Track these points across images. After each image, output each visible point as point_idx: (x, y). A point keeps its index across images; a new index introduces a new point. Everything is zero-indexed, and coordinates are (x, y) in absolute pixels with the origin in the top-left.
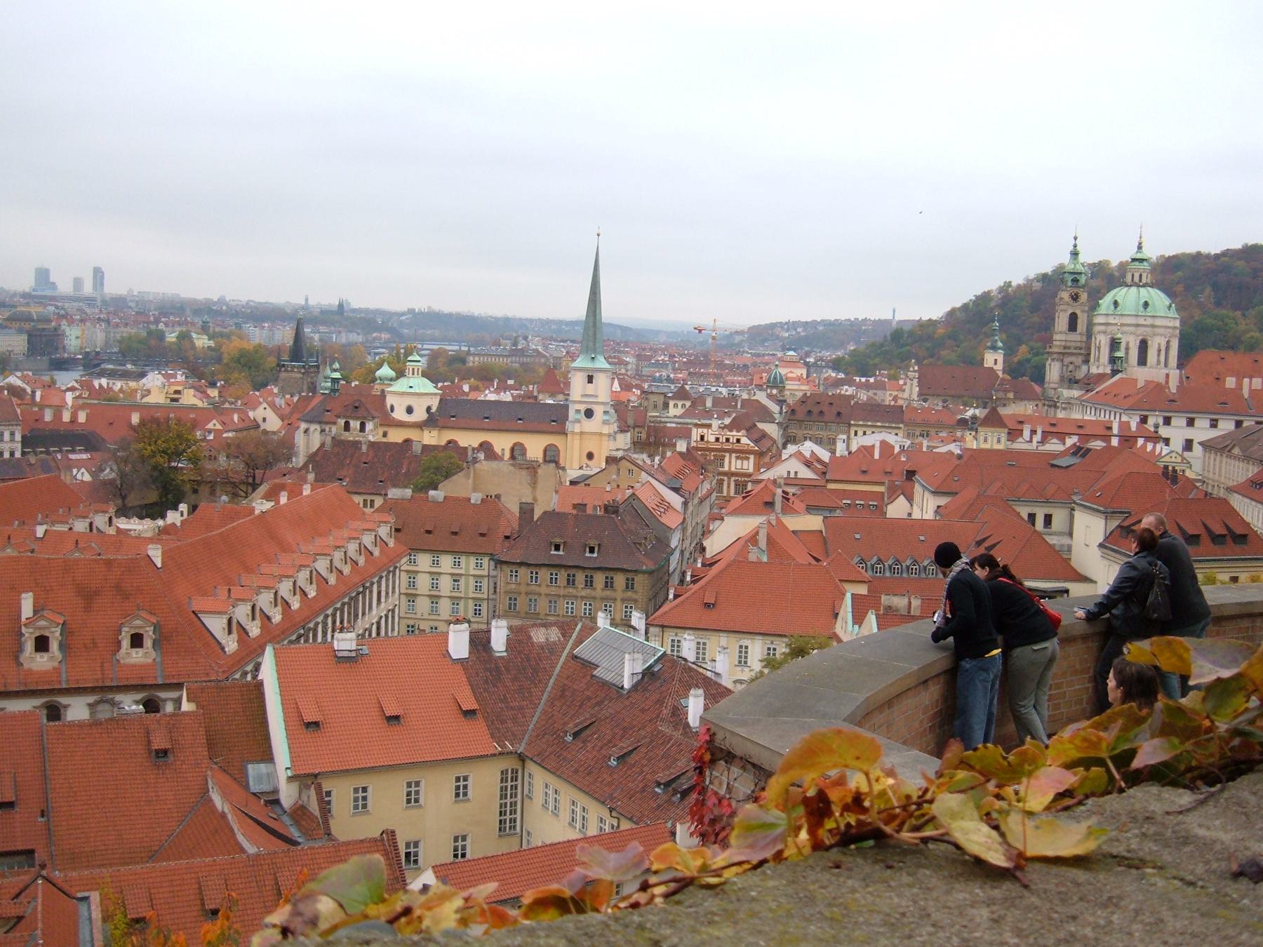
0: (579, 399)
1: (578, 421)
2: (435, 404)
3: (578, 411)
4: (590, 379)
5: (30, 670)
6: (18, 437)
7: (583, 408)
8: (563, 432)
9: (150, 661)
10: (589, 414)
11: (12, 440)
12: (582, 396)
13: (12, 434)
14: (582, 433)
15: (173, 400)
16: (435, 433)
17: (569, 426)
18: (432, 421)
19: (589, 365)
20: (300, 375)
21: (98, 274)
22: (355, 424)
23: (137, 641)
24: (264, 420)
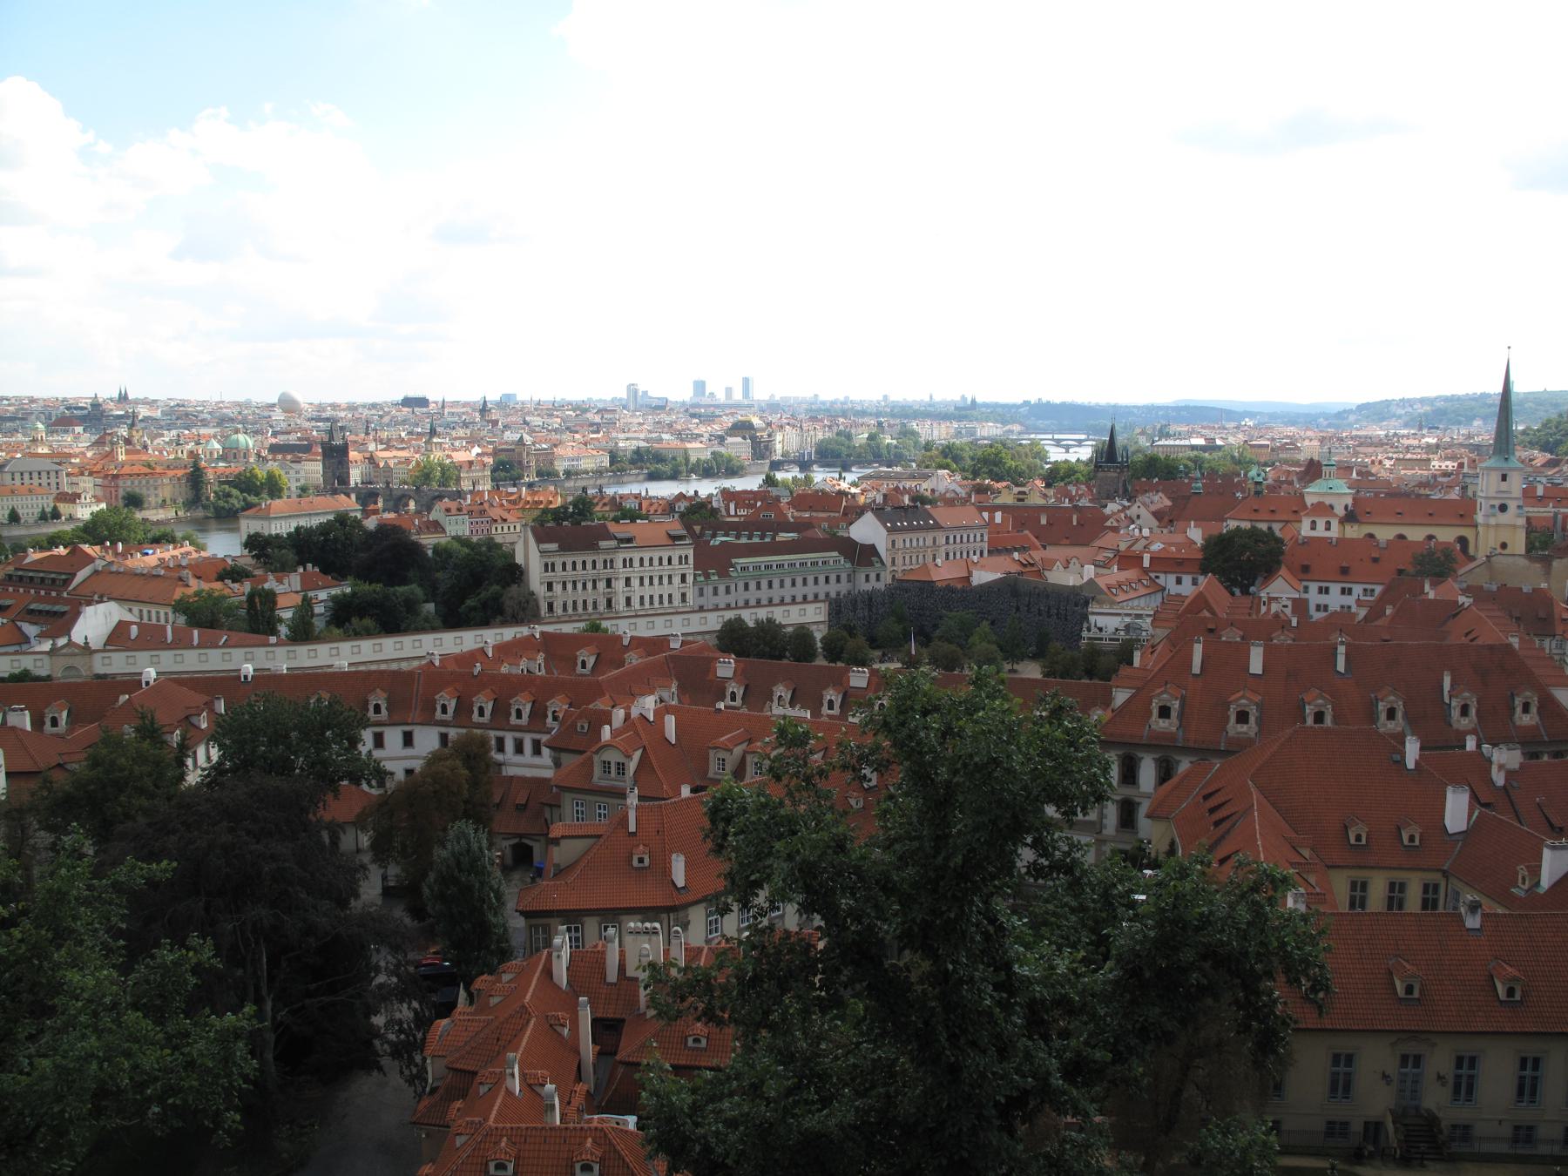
0: (1494, 495)
1: (1494, 515)
2: (1349, 501)
3: (1493, 506)
4: (1504, 478)
5: (1457, 730)
6: (986, 538)
7: (1497, 503)
8: (1476, 526)
9: (1534, 723)
10: (1503, 508)
11: (982, 540)
12: (1497, 492)
13: (982, 535)
14: (1497, 526)
15: (1019, 500)
16: (1356, 527)
17: (1480, 518)
18: (1350, 517)
19: (1504, 465)
20: (1116, 475)
21: (746, 382)
22: (1321, 524)
23: (1526, 708)
24: (1138, 517)
